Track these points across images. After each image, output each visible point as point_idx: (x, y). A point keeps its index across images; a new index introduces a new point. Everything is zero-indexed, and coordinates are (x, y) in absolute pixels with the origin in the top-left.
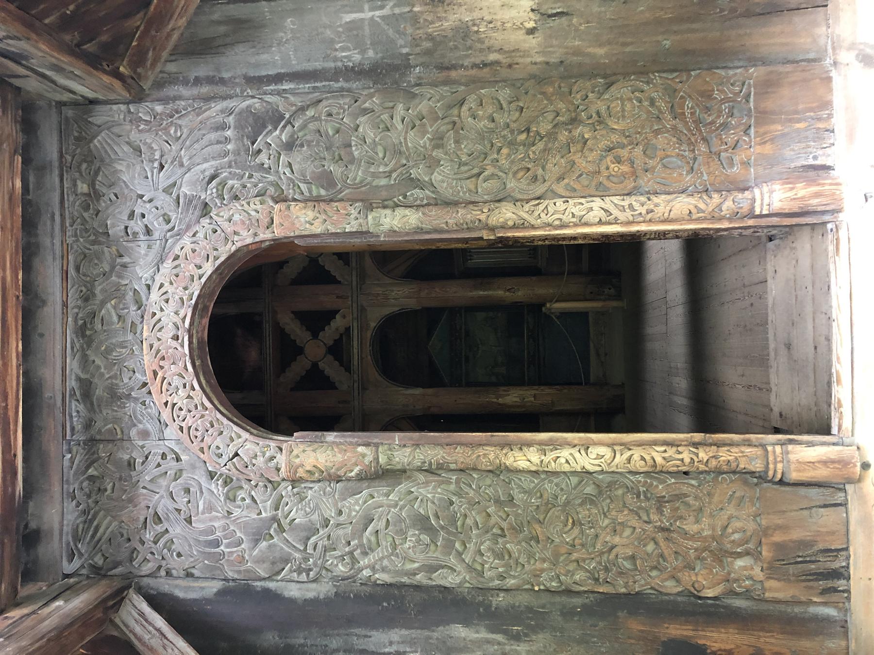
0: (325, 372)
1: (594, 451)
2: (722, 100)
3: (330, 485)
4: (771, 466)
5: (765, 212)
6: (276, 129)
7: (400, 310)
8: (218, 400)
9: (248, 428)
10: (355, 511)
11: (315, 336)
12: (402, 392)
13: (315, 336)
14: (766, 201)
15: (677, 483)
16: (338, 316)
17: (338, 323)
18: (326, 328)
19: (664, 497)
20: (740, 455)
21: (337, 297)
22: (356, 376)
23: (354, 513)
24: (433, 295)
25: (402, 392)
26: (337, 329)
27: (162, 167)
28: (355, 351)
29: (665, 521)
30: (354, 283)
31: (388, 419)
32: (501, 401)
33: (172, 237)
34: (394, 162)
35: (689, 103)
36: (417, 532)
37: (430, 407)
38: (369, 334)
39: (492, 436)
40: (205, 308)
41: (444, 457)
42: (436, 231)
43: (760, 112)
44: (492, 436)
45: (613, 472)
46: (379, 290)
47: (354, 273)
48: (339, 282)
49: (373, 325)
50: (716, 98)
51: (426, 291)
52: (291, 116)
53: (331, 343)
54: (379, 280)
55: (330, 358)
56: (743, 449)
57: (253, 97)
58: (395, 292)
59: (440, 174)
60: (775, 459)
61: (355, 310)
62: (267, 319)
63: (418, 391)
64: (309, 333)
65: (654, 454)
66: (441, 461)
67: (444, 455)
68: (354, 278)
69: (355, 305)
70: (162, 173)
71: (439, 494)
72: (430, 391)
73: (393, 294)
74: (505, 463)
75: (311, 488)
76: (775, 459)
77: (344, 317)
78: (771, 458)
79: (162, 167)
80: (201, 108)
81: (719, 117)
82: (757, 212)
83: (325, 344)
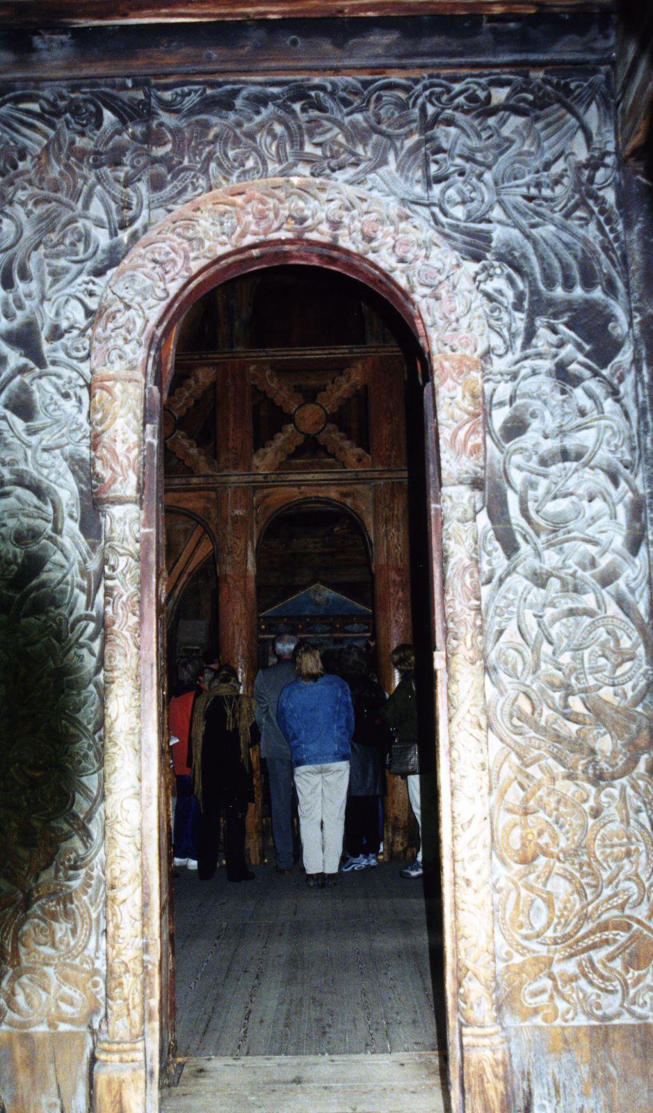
0: (279, 434)
1: (132, 805)
2: (625, 981)
3: (84, 437)
4: (115, 1047)
5: (465, 1041)
6: (587, 356)
7: (370, 541)
8: (204, 281)
9: (165, 324)
10: (49, 474)
12: (250, 543)
13: (330, 418)
14: (481, 1041)
15: (91, 920)
16: (359, 451)
17: (352, 452)
18: (342, 434)
19: (72, 902)
20: (131, 1007)
23: (45, 472)
24: (392, 590)
26: (341, 449)
27: (530, 199)
28: (310, 477)
29: (39, 902)
33: (433, 214)
34: (542, 523)
35: (623, 937)
36: (20, 560)
39: (152, 666)
40: (333, 261)
41: (121, 596)
42: (443, 582)
43: (606, 1035)
44: (152, 666)
45: (105, 833)
50: (628, 972)
51: (398, 579)
52: (604, 377)
55: (300, 440)
56: (139, 1009)
57: (630, 325)
58: (396, 534)
59: (525, 589)
60: (125, 1051)
62: (355, 350)
65: (129, 889)
66: (115, 593)
67: (124, 598)
70: (520, 199)
71: (72, 590)
72: (252, 585)
74: (113, 682)
75: (80, 411)
76: (125, 1051)
78: (127, 1046)
79: (530, 199)
80: (614, 252)
81: (602, 977)
82: (465, 1030)
83: (319, 433)
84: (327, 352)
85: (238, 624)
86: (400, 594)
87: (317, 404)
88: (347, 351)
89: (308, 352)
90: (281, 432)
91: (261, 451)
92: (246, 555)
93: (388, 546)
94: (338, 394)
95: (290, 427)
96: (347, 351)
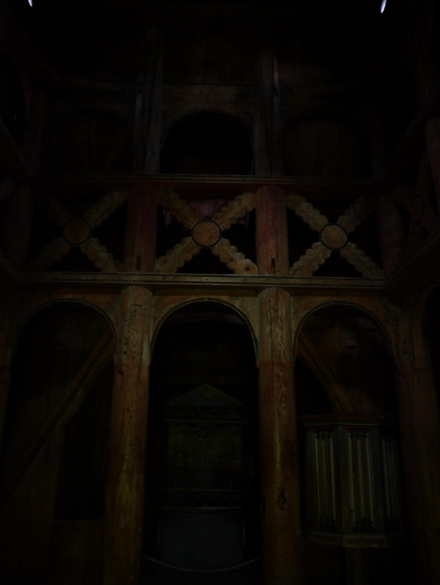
0: (179, 245)
7: (256, 339)
11: (225, 234)
13: (225, 234)
16: (248, 261)
18: (233, 247)
21: (273, 260)
22: (171, 278)
24: (275, 385)
25: (146, 336)
26: (232, 260)
28: (204, 279)
30: (292, 281)
31: (112, 318)
32: (124, 477)
37: (122, 373)
38: (224, 298)
46: (282, 312)
47: (305, 282)
48: (291, 264)
49: (237, 303)
51: (281, 374)
53: (215, 251)
54: (296, 312)
55: (197, 250)
58: (280, 333)
61: (257, 280)
62: (246, 179)
63: (146, 358)
64: (228, 227)
68: (297, 281)
69: (263, 280)
72: (145, 374)
73: (278, 330)
77: (247, 269)
83: (215, 244)
84: (223, 179)
85: (128, 410)
86: (283, 389)
87: (213, 222)
88: (240, 179)
89: (208, 178)
90: (180, 243)
91: (162, 258)
92: (141, 347)
93: (272, 343)
94: (231, 215)
95: (188, 240)
96: (240, 179)
